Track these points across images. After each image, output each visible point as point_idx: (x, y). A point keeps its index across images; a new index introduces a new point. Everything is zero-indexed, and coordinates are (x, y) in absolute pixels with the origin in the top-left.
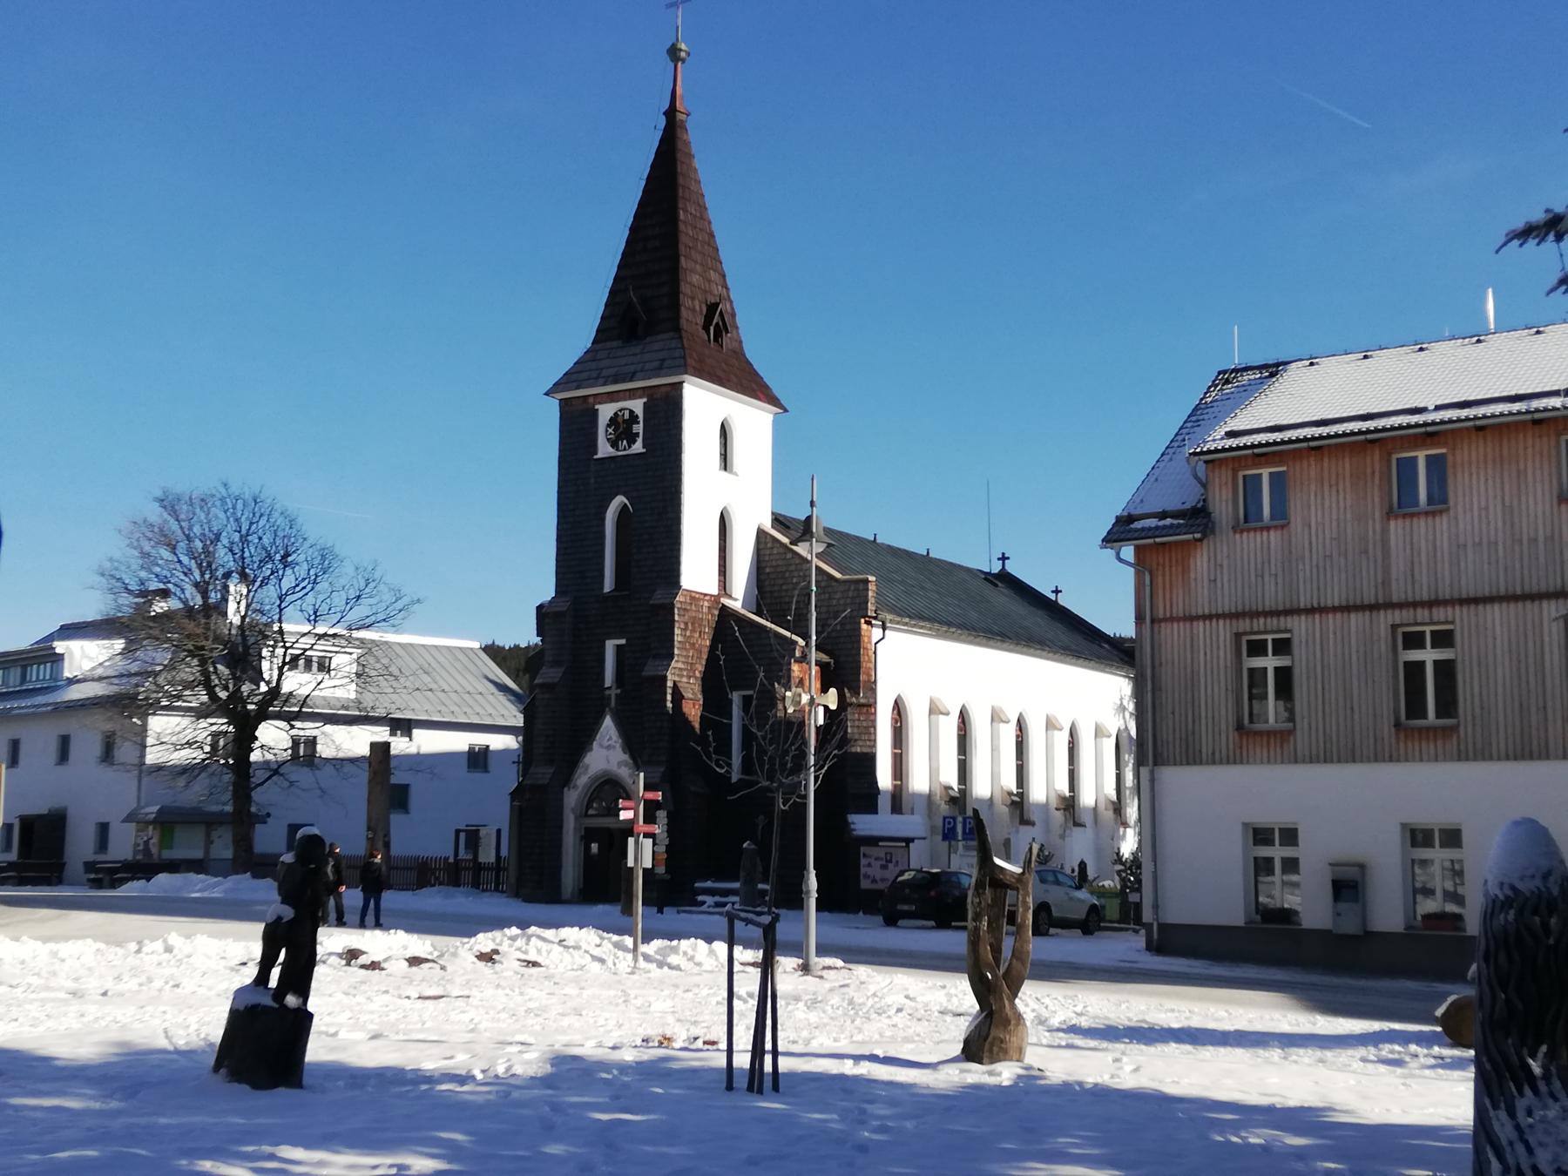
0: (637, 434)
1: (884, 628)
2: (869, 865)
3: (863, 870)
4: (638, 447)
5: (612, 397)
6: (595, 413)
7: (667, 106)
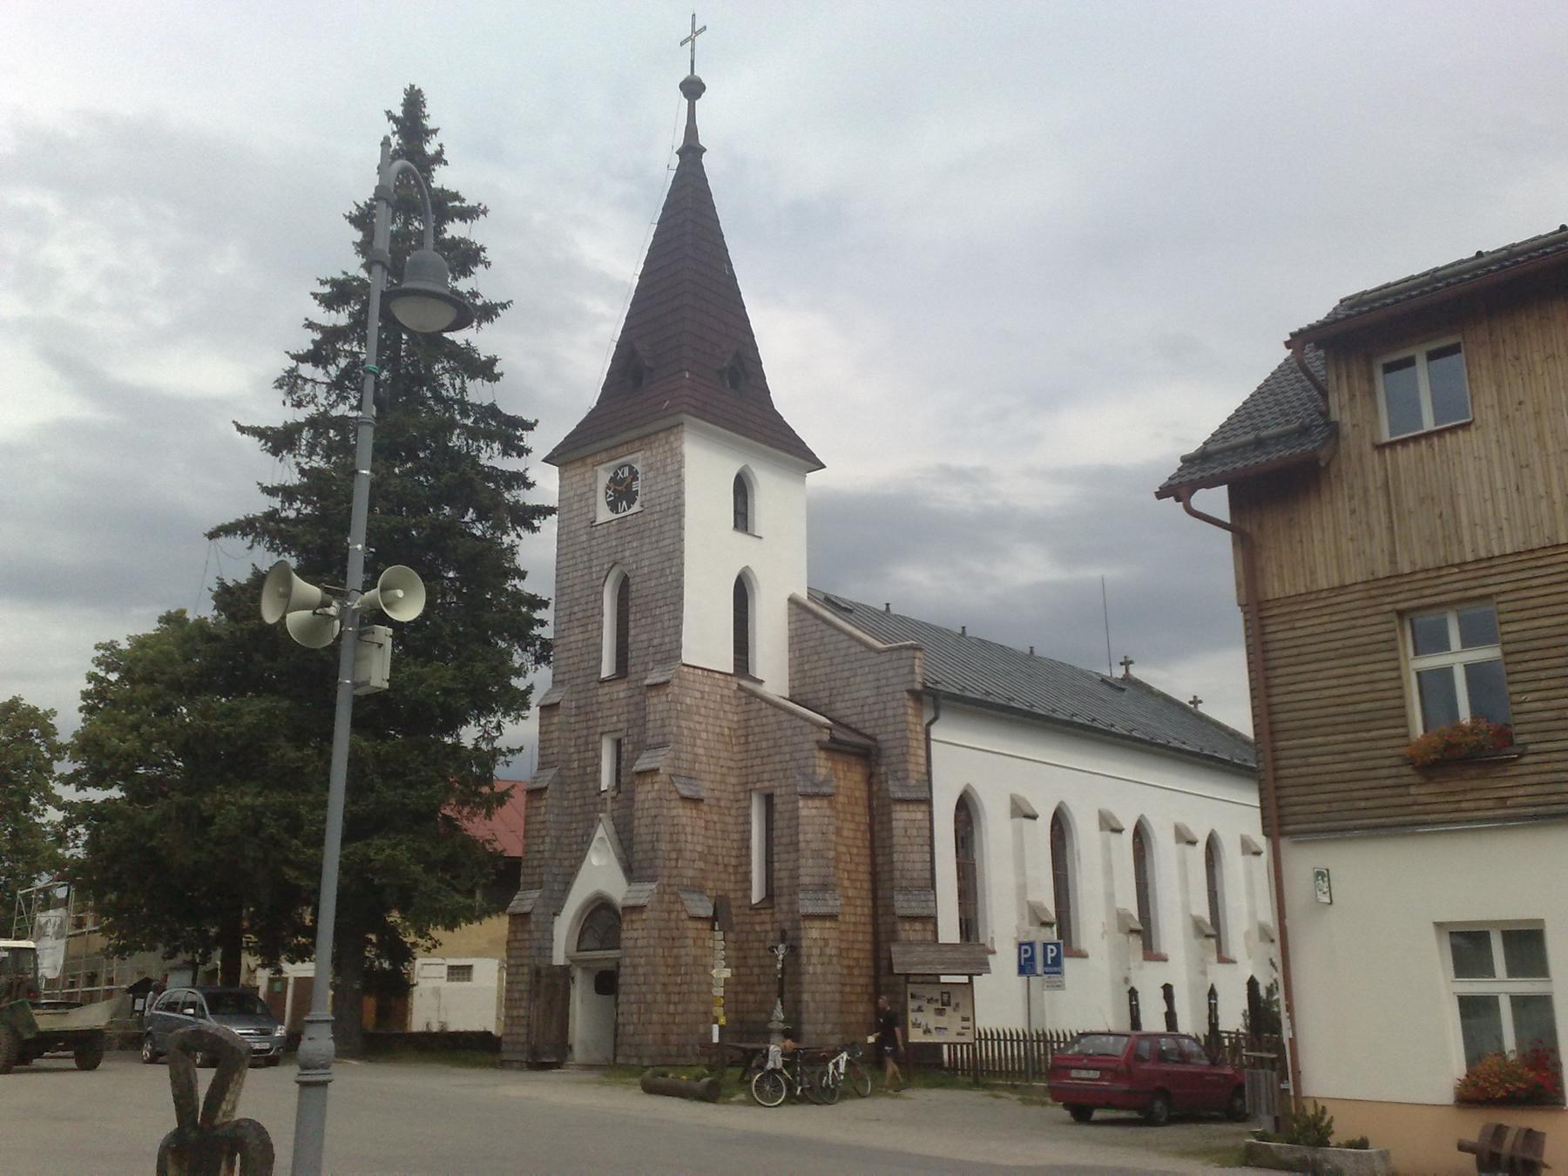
1: (937, 709)
2: (920, 1009)
3: (912, 1017)
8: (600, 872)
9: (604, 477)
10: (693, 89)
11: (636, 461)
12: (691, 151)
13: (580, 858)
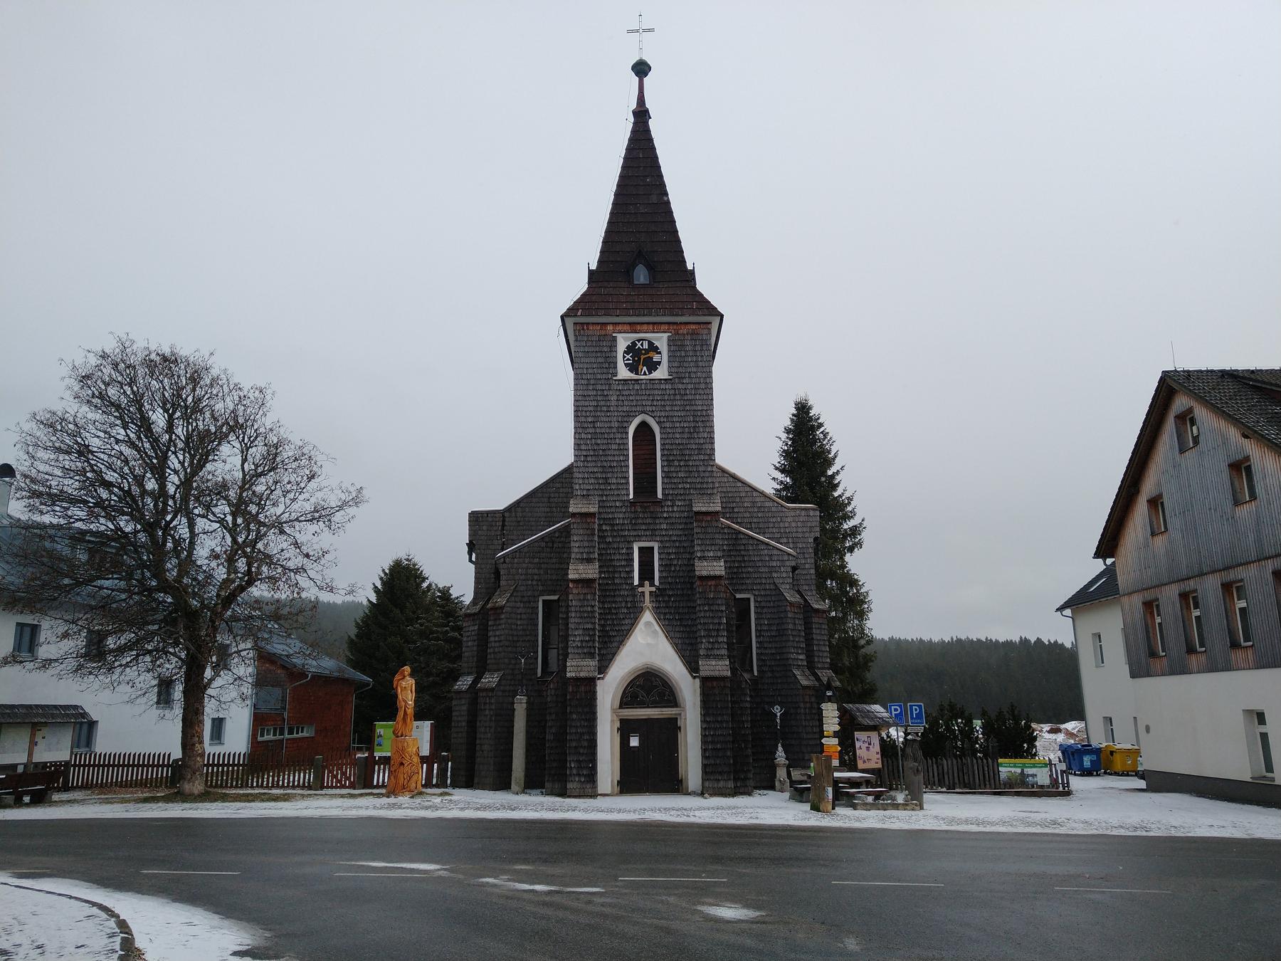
0: (659, 363)
4: (661, 373)
5: (633, 327)
6: (615, 339)
7: (634, 106)
8: (648, 646)
9: (623, 342)
10: (641, 69)
11: (658, 339)
12: (641, 115)
13: (625, 634)
